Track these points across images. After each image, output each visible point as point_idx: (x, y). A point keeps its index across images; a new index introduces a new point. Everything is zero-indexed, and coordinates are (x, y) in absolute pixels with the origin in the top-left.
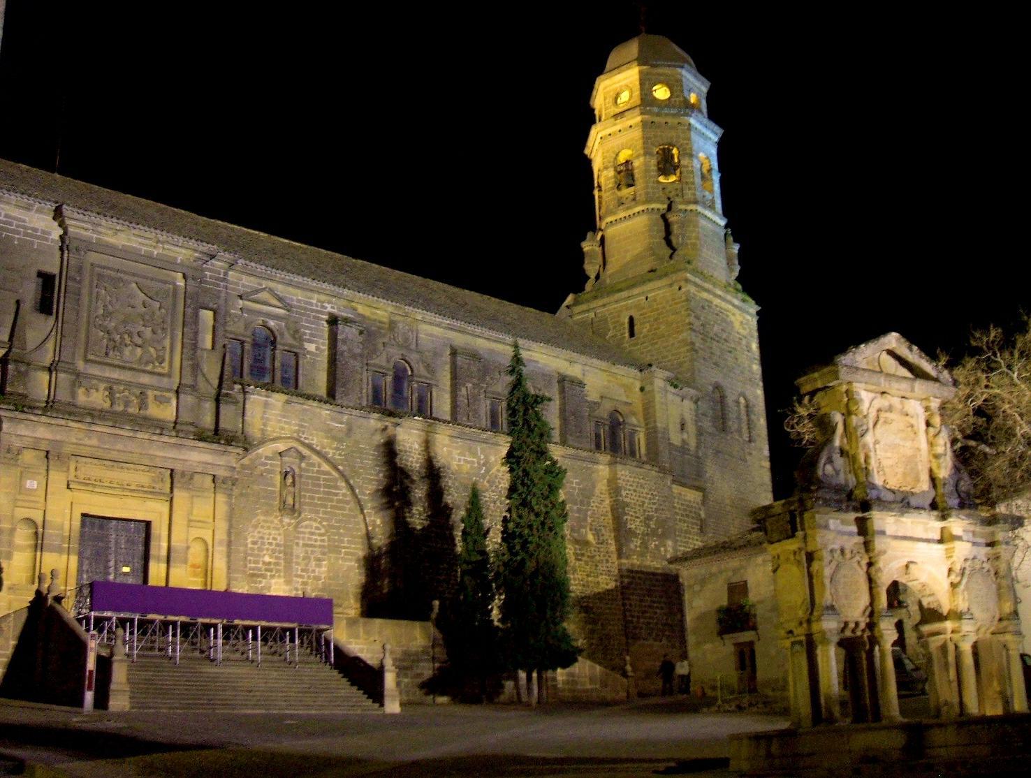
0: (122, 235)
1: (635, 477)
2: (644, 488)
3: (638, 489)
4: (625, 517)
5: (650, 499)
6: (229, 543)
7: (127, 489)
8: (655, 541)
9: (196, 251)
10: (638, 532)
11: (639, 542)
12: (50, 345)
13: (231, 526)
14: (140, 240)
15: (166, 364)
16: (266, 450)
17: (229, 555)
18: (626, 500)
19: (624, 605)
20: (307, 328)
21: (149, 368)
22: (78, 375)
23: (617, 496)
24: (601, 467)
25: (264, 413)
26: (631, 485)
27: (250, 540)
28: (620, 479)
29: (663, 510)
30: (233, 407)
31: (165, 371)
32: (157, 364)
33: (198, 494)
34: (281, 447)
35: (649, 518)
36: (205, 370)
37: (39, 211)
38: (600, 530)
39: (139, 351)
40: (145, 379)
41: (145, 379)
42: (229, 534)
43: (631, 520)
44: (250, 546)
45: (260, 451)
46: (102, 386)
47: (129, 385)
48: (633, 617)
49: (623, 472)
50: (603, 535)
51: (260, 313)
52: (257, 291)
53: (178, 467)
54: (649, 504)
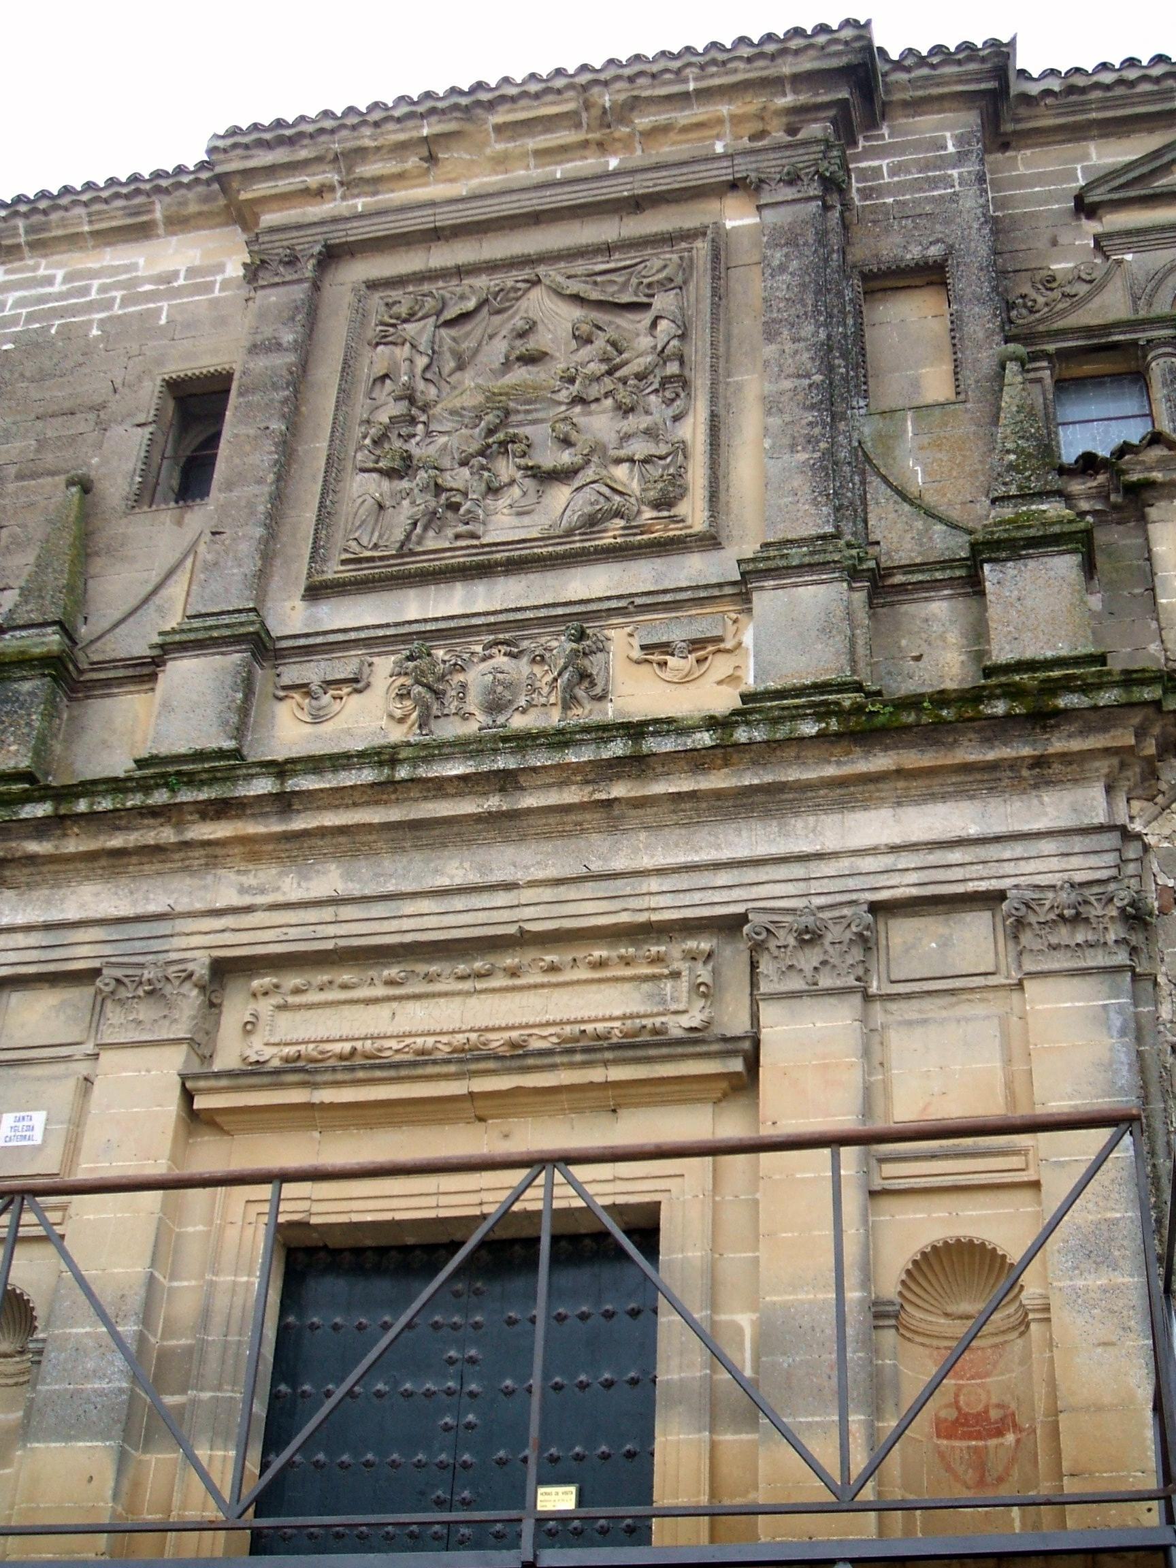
0: (451, 156)
9: (773, 84)
12: (177, 589)
14: (533, 143)
21: (612, 533)
33: (909, 1010)
36: (916, 474)
37: (178, 223)
39: (560, 495)
46: (384, 665)
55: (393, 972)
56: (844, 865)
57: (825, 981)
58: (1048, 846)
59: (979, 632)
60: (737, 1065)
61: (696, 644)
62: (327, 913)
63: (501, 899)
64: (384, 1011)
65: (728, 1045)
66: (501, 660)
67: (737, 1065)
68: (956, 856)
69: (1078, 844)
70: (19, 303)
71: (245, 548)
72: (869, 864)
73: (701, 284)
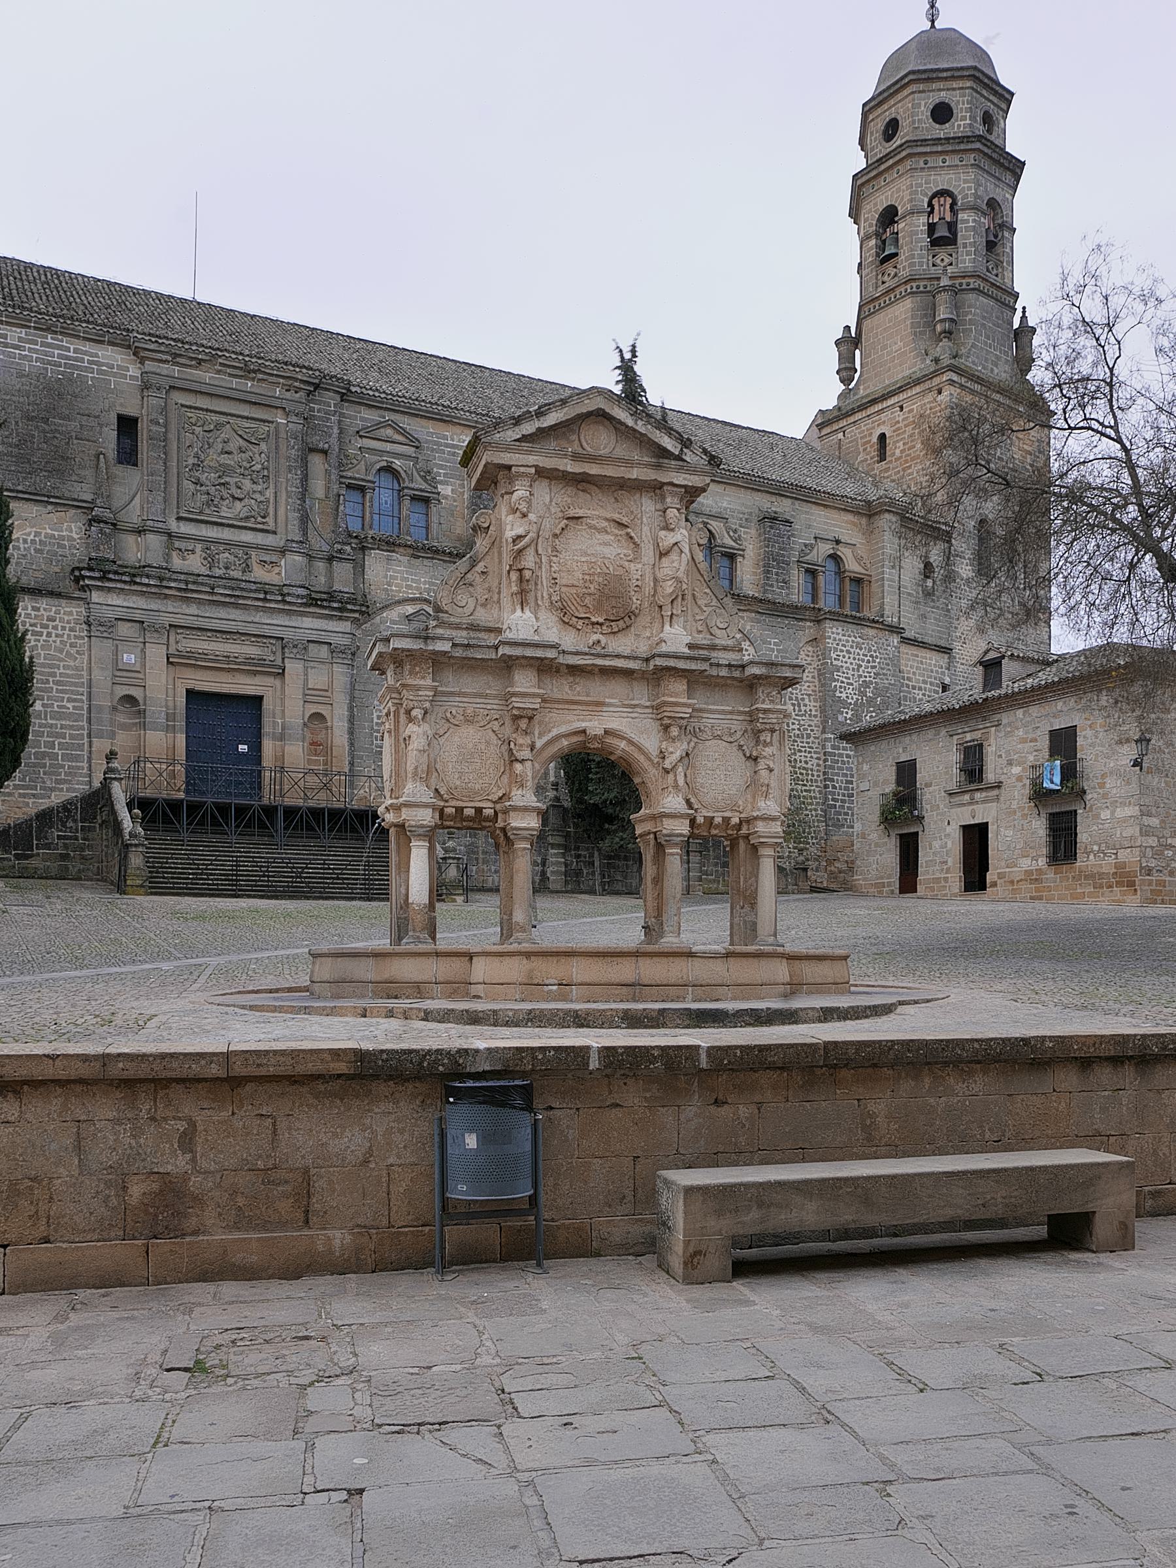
1: (850, 636)
2: (861, 649)
3: (852, 650)
4: (834, 684)
5: (868, 662)
6: (351, 720)
7: (228, 665)
8: (872, 712)
10: (849, 701)
11: (850, 713)
12: (137, 499)
13: (352, 699)
15: (270, 520)
16: (394, 614)
17: (351, 732)
18: (835, 663)
19: (826, 787)
20: (441, 467)
22: (170, 535)
23: (824, 659)
24: (808, 624)
25: (388, 570)
26: (843, 645)
27: (375, 715)
28: (830, 638)
29: (884, 674)
30: (349, 566)
31: (271, 527)
32: (259, 518)
33: (312, 664)
34: (410, 609)
35: (866, 684)
38: (803, 699)
39: (238, 504)
40: (247, 537)
41: (247, 537)
42: (351, 708)
43: (841, 687)
44: (375, 720)
45: (385, 615)
46: (199, 547)
47: (229, 545)
48: (837, 800)
49: (834, 630)
50: (805, 705)
51: (382, 452)
52: (379, 425)
53: (287, 634)
54: (867, 667)
55: (209, 634)
56: (302, 631)
57: (298, 656)
58: (340, 635)
59: (330, 574)
60: (281, 671)
61: (272, 563)
62: (195, 618)
63: (233, 623)
64: (207, 643)
65: (280, 667)
66: (227, 555)
67: (281, 671)
68: (323, 633)
69: (347, 636)
70: (60, 355)
71: (160, 499)
72: (306, 631)
73: (272, 440)
